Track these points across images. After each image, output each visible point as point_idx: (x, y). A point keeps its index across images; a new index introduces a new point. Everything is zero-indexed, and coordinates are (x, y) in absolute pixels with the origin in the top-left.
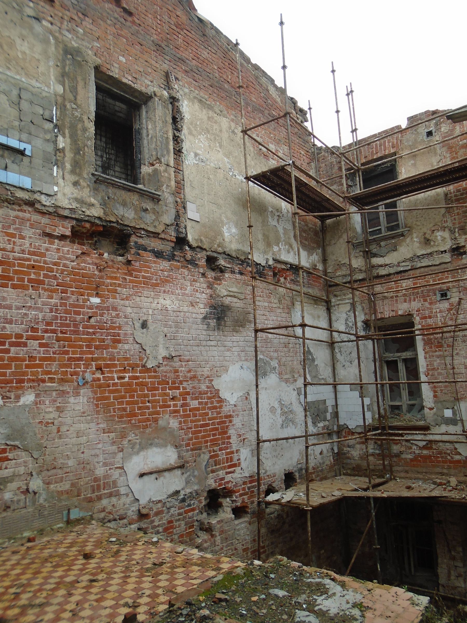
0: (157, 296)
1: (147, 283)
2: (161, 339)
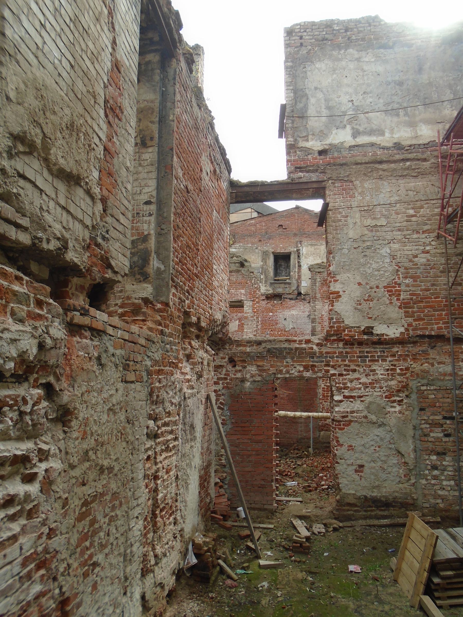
0: (290, 311)
1: (287, 308)
2: (291, 323)
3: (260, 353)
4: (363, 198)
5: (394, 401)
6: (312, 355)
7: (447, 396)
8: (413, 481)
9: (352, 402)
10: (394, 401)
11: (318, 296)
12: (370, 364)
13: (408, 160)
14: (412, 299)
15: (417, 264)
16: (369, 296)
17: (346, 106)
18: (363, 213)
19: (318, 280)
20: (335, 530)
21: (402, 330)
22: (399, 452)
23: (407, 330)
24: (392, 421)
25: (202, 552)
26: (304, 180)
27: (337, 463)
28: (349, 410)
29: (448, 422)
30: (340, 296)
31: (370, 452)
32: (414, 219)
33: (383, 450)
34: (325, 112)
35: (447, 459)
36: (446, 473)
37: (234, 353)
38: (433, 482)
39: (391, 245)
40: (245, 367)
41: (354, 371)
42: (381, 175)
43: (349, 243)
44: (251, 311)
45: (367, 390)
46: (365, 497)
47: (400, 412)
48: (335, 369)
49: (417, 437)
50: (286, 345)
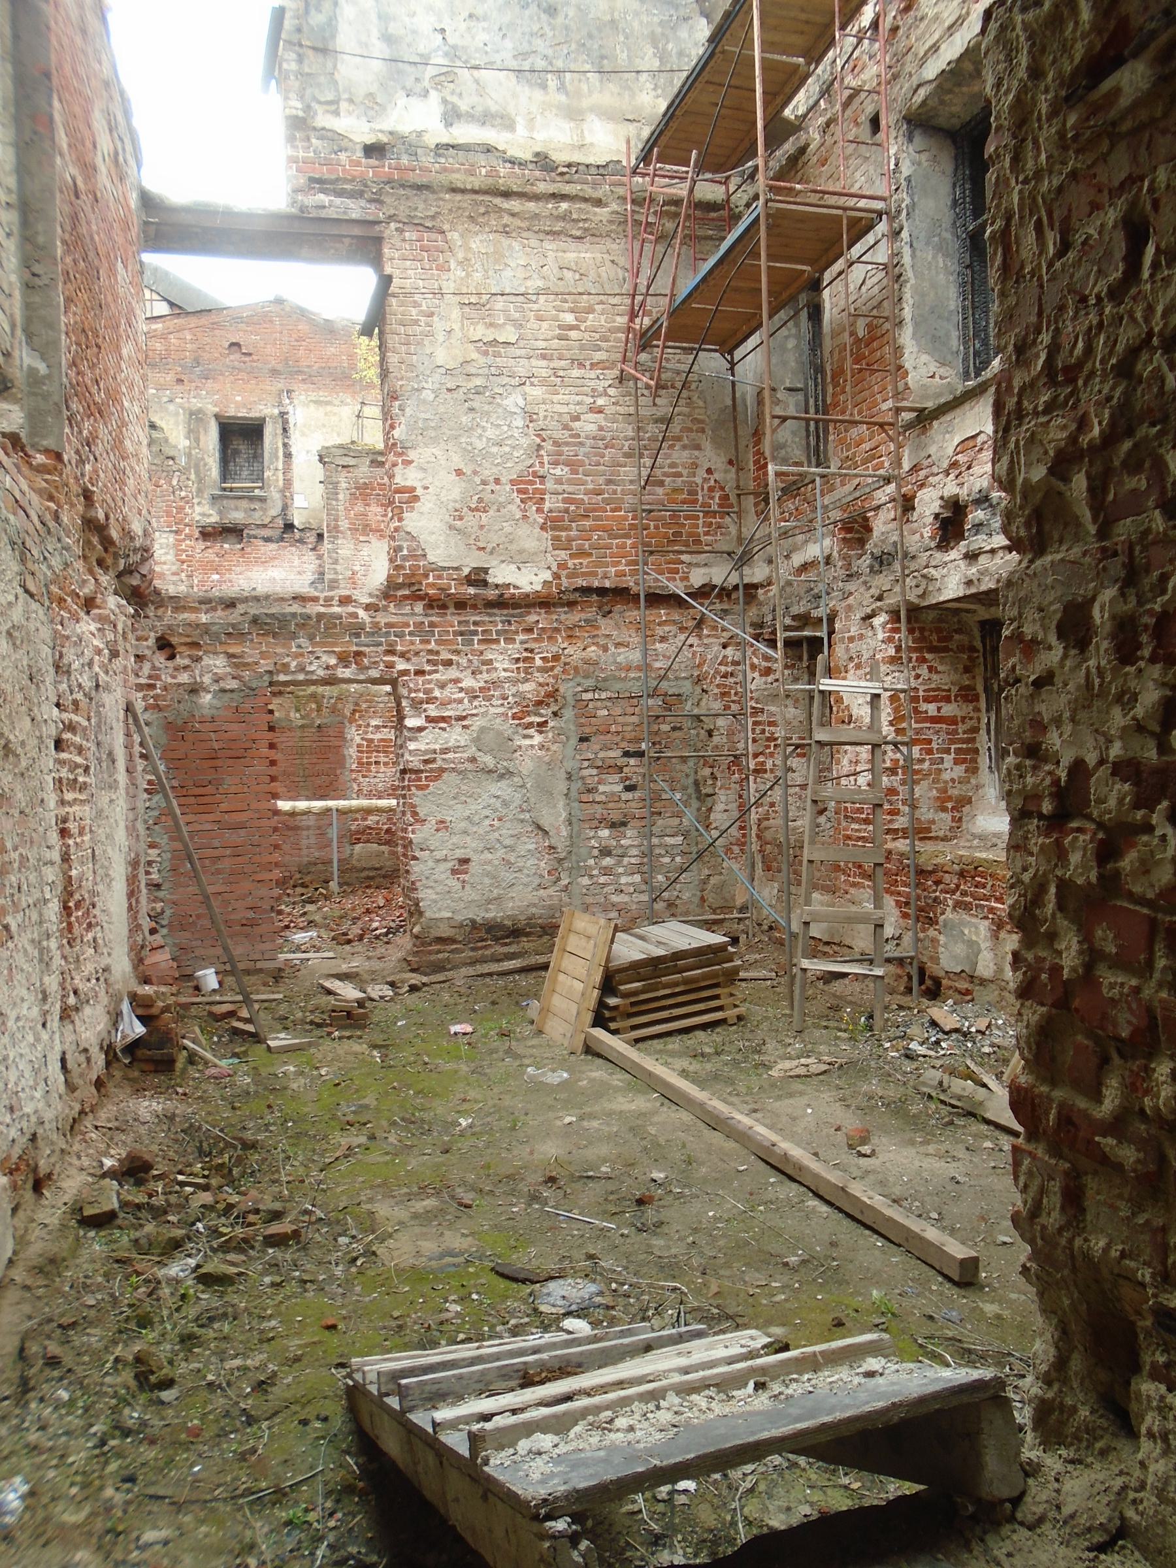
3: (233, 626)
4: (468, 275)
5: (530, 725)
6: (356, 630)
7: (631, 710)
8: (565, 882)
9: (444, 729)
10: (530, 725)
11: (344, 524)
12: (482, 647)
13: (564, 197)
14: (567, 511)
15: (579, 436)
16: (480, 500)
17: (429, 43)
18: (467, 309)
19: (344, 485)
20: (413, 989)
21: (547, 576)
22: (539, 827)
23: (557, 576)
24: (526, 765)
25: (154, 1011)
26: (331, 213)
27: (415, 858)
28: (437, 747)
29: (632, 761)
30: (416, 498)
31: (481, 831)
32: (573, 334)
33: (508, 825)
34: (379, 48)
35: (629, 833)
36: (626, 860)
37: (170, 627)
38: (602, 880)
39: (527, 388)
40: (198, 659)
41: (449, 663)
42: (506, 226)
43: (437, 377)
44: (170, 557)
45: (476, 703)
46: (473, 922)
47: (541, 747)
48: (408, 660)
49: (574, 794)
50: (296, 608)
